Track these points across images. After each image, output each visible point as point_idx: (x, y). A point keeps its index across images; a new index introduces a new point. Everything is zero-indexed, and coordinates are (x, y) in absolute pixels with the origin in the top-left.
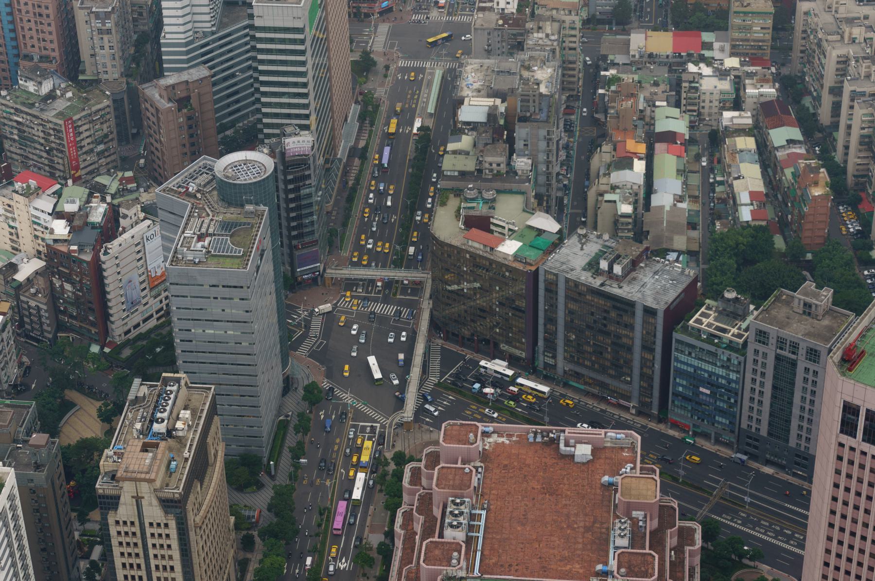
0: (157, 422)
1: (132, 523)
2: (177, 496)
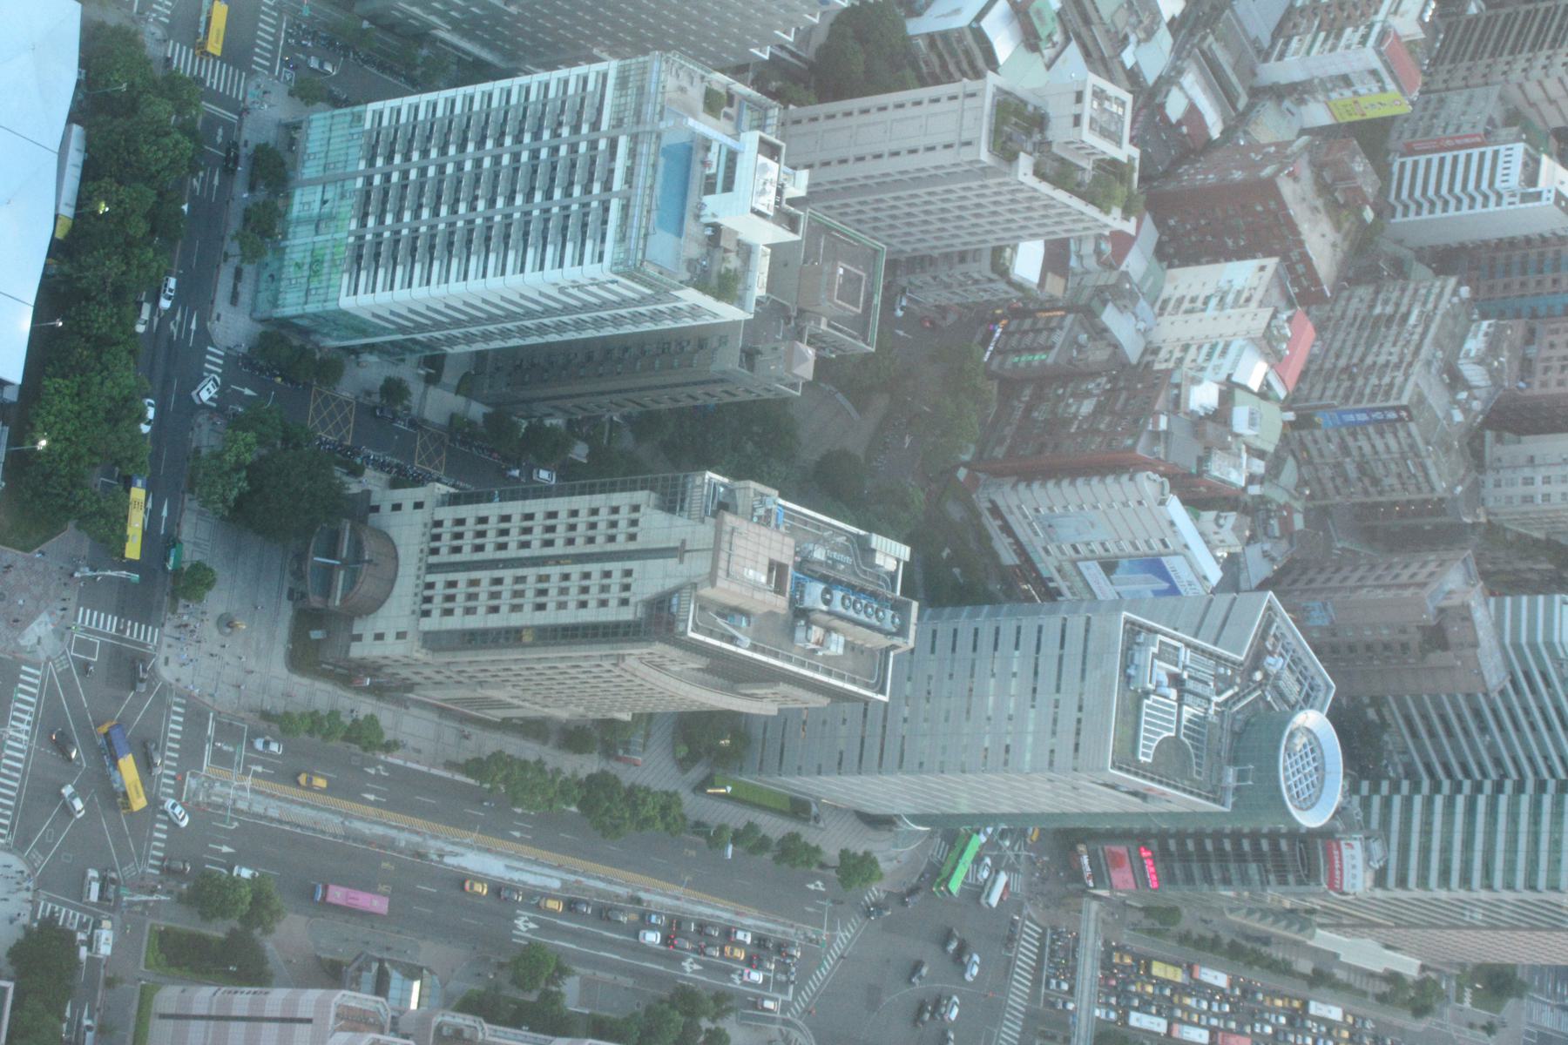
0: (827, 591)
1: (632, 537)
2: (681, 628)
